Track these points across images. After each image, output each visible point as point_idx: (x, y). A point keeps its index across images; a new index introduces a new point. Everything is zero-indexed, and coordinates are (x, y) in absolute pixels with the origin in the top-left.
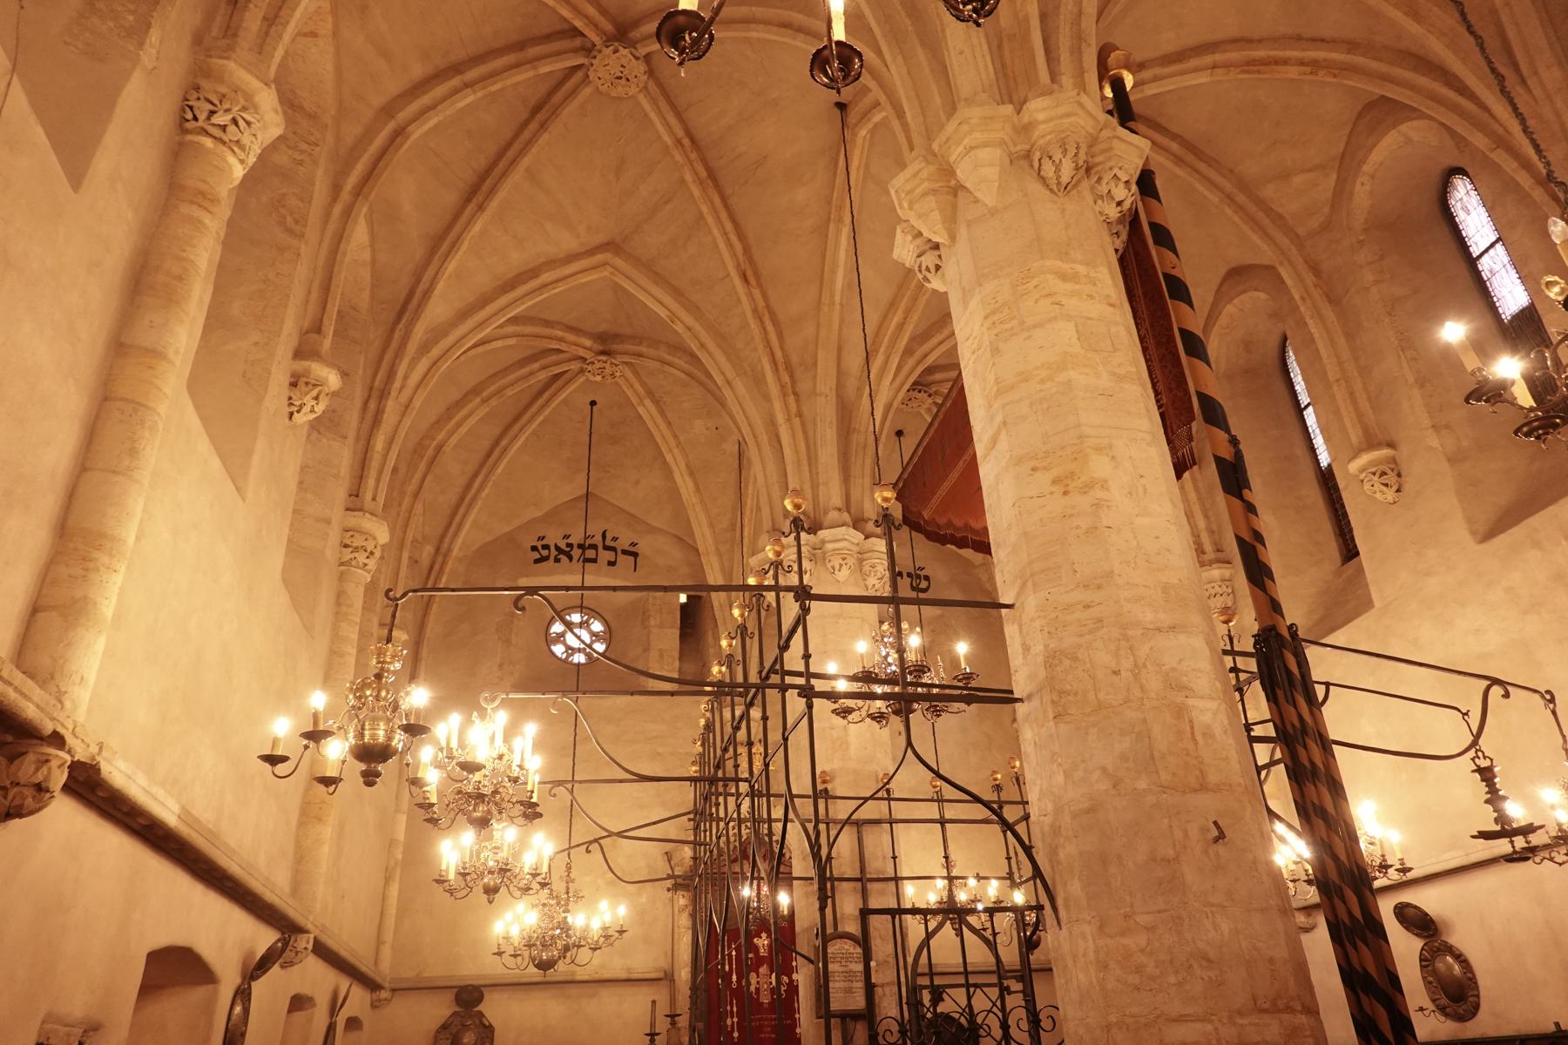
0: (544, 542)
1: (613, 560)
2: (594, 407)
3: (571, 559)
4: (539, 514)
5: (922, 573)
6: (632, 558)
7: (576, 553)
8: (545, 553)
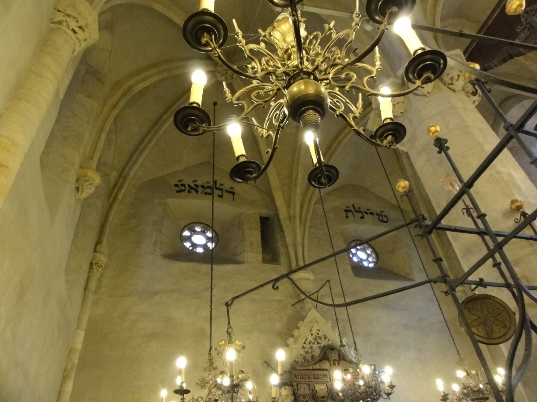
0: (182, 183)
1: (221, 194)
2: (216, 107)
3: (197, 192)
4: (181, 168)
5: (383, 214)
6: (231, 195)
7: (200, 189)
8: (183, 188)
